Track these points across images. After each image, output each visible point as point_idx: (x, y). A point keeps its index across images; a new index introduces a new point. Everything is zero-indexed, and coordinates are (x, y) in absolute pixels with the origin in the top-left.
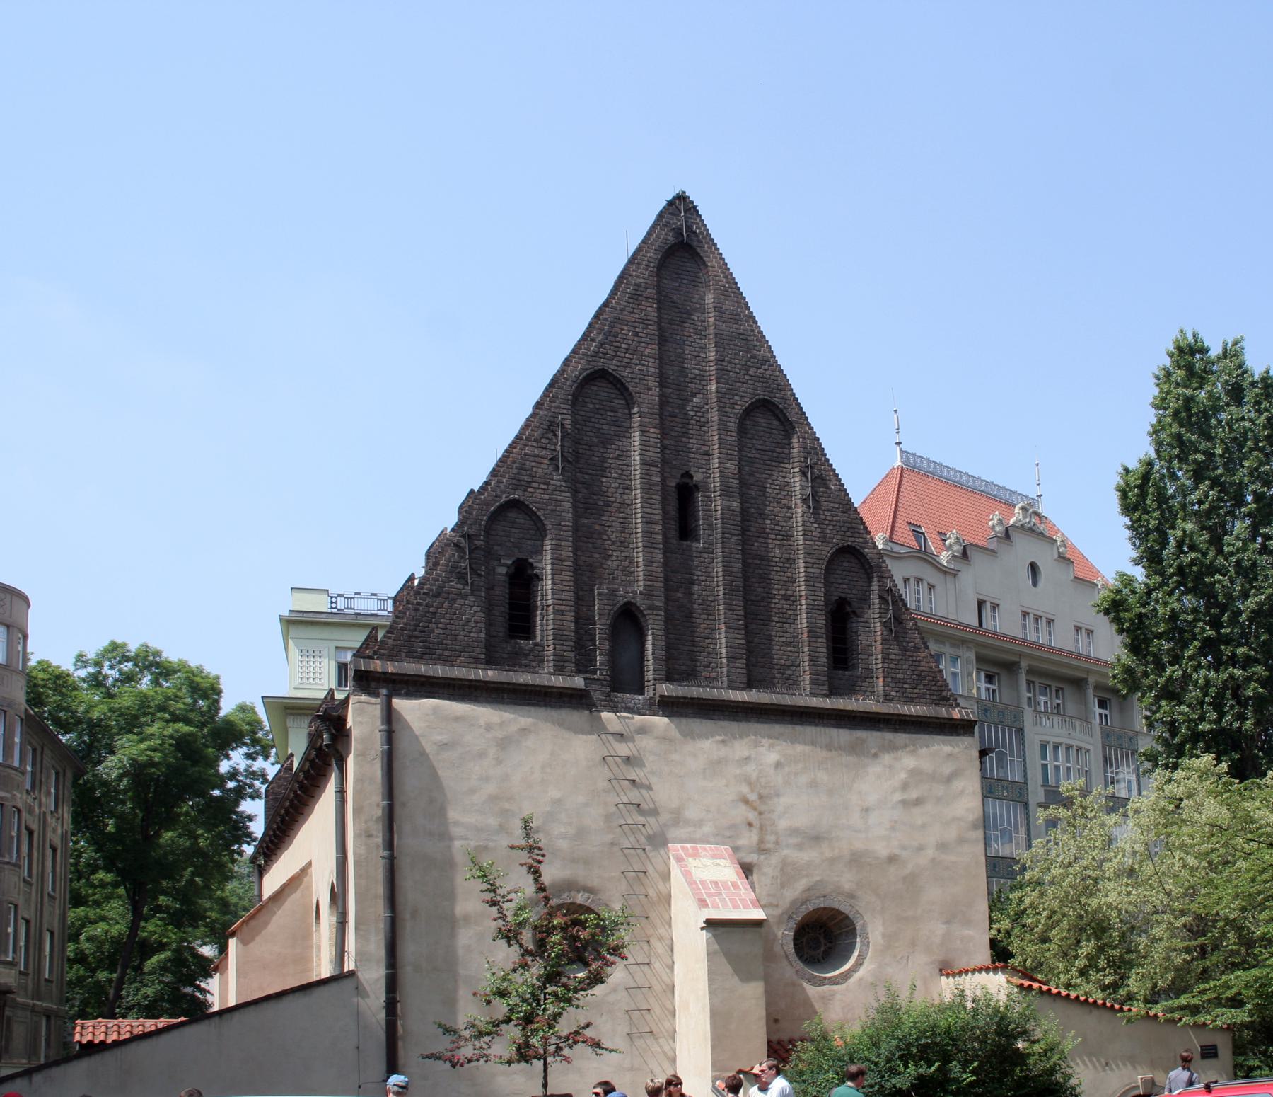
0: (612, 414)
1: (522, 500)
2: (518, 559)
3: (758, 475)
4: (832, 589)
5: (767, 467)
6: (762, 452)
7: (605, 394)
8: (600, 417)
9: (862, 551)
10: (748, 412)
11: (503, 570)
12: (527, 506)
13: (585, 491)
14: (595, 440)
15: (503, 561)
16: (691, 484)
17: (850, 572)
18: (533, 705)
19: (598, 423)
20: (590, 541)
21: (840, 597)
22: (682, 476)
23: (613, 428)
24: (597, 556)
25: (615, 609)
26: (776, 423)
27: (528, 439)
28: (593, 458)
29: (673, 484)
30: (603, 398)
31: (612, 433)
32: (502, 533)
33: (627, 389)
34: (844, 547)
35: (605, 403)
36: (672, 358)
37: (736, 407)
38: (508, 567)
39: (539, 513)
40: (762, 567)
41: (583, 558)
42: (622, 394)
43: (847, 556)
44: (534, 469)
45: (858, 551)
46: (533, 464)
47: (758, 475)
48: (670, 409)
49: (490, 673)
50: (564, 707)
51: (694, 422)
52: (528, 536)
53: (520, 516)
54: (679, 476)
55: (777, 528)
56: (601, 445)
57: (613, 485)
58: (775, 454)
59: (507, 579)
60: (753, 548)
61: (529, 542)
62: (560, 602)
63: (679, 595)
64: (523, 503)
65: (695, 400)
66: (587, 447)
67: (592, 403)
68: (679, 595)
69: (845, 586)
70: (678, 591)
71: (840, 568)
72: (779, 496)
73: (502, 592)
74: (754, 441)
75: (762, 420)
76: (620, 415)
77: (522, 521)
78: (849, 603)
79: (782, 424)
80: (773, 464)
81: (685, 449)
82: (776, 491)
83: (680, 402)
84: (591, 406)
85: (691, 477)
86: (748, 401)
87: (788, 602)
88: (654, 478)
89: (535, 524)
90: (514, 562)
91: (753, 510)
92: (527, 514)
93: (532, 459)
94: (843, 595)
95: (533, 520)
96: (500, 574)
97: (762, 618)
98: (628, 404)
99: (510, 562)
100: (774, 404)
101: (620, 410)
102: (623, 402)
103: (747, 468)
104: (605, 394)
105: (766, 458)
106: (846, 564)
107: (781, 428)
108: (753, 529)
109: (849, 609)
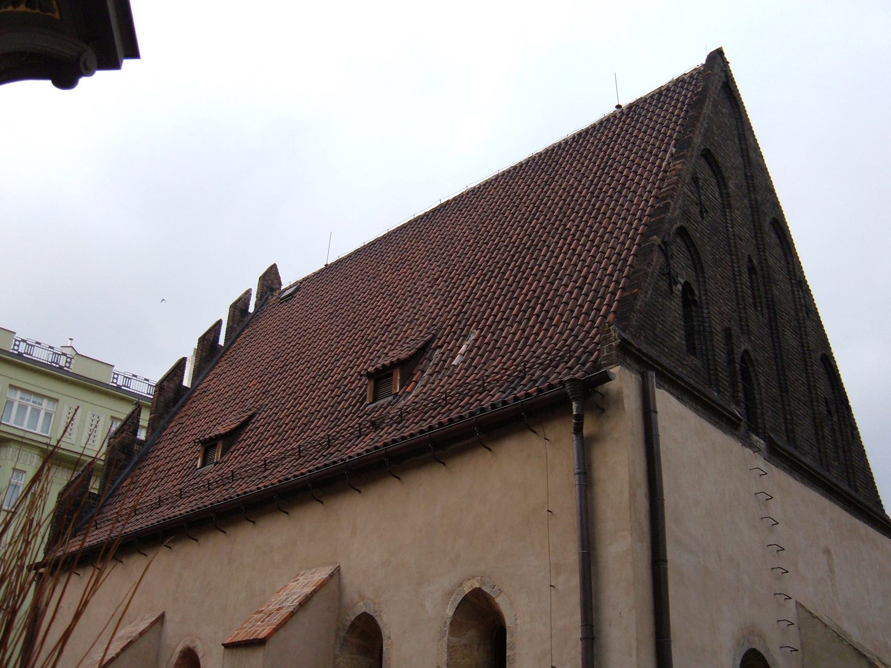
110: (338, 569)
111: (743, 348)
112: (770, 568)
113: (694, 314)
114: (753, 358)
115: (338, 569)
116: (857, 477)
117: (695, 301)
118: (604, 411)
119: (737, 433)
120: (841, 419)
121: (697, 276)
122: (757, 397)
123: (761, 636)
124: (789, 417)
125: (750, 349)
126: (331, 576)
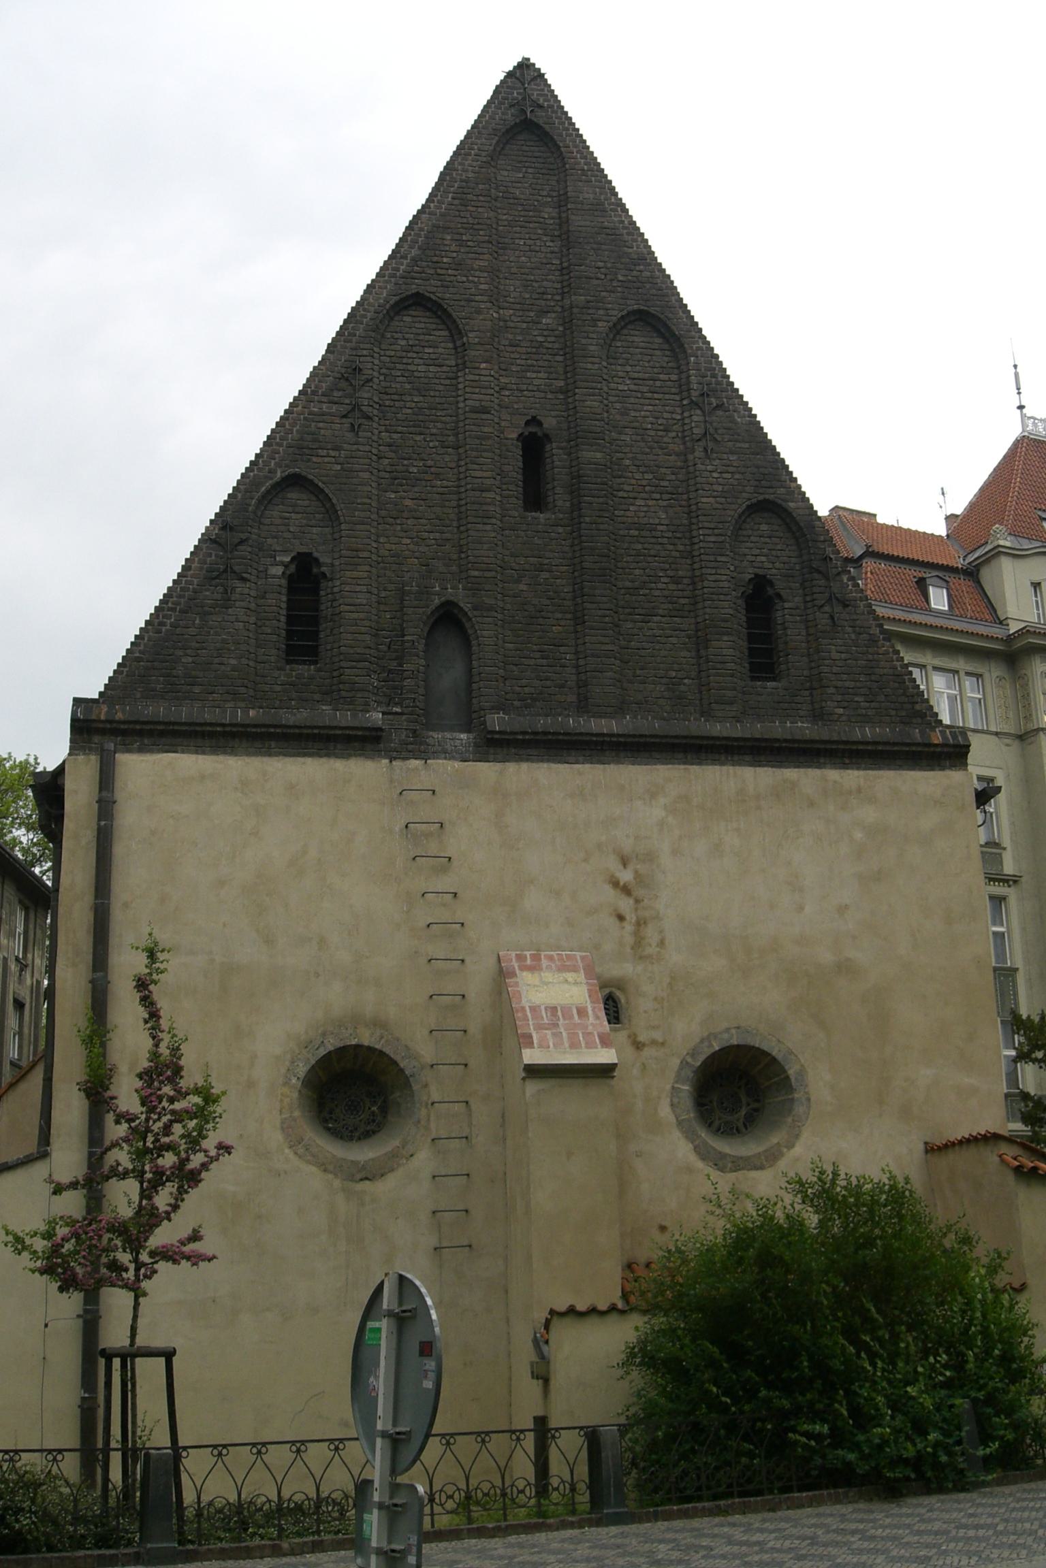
0: (431, 350)
1: (304, 474)
2: (298, 553)
3: (633, 414)
4: (745, 563)
5: (647, 401)
6: (641, 382)
7: (422, 325)
8: (415, 355)
9: (784, 504)
10: (617, 329)
11: (279, 570)
12: (311, 482)
13: (392, 455)
14: (407, 386)
15: (278, 559)
16: (540, 434)
17: (770, 537)
19: (412, 363)
20: (398, 522)
21: (756, 575)
22: (528, 423)
23: (432, 369)
24: (408, 541)
25: (429, 611)
26: (659, 340)
27: (314, 393)
28: (405, 411)
29: (515, 436)
30: (420, 331)
31: (431, 375)
32: (279, 521)
33: (450, 316)
34: (759, 502)
35: (422, 337)
36: (514, 270)
37: (600, 324)
38: (286, 566)
39: (327, 491)
40: (642, 540)
41: (388, 546)
42: (444, 323)
43: (766, 515)
44: (322, 432)
45: (780, 506)
46: (321, 425)
47: (633, 414)
48: (510, 336)
49: (252, 713)
50: (356, 756)
51: (544, 351)
52: (313, 522)
53: (304, 496)
54: (523, 423)
55: (663, 483)
56: (416, 393)
57: (431, 444)
58: (658, 383)
59: (284, 582)
60: (628, 513)
61: (315, 530)
63: (523, 587)
64: (305, 479)
65: (544, 321)
66: (396, 397)
67: (404, 339)
68: (523, 587)
69: (763, 559)
70: (518, 581)
71: (756, 533)
72: (665, 439)
73: (278, 602)
74: (629, 368)
75: (639, 338)
76: (440, 350)
77: (306, 503)
78: (771, 583)
79: (667, 341)
80: (656, 396)
81: (530, 388)
82: (660, 433)
83: (525, 325)
84: (403, 343)
85: (540, 424)
86: (616, 314)
87: (680, 586)
88: (486, 429)
89: (324, 506)
90: (293, 559)
91: (627, 462)
92: (312, 492)
93: (317, 418)
94: (760, 572)
95: (319, 500)
96: (274, 577)
97: (641, 611)
98: (452, 336)
99: (287, 559)
100: (653, 316)
101: (442, 344)
102: (446, 333)
103: (618, 406)
104: (422, 325)
105: (645, 389)
106: (764, 527)
107: (666, 346)
108: (626, 487)
109: (770, 591)
111: (437, 602)
117: (324, 574)
120: (808, 598)
123: (378, 1023)
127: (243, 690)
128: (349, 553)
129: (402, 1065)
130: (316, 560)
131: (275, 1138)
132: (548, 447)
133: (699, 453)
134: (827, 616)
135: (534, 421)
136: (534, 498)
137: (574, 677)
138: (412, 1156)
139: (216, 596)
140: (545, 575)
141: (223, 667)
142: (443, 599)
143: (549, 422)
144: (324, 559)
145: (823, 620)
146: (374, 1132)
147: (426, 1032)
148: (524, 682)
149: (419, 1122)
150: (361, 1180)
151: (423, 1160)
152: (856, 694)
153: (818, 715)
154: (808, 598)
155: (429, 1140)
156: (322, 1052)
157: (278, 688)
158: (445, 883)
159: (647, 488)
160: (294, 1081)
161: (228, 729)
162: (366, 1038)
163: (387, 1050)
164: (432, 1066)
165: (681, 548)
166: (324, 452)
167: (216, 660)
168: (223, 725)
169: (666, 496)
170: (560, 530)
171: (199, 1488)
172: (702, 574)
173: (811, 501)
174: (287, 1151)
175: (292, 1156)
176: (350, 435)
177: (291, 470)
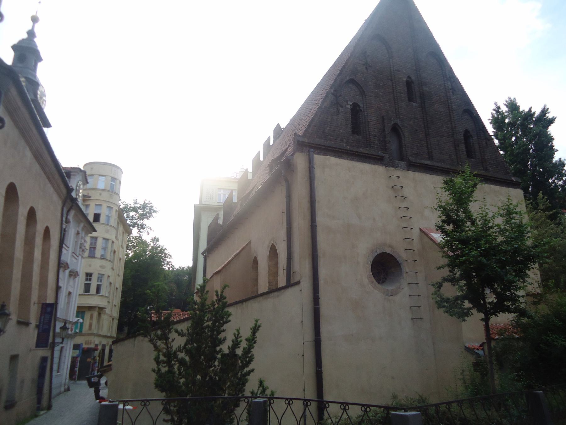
2: (354, 102)
11: (349, 107)
15: (349, 103)
18: (365, 162)
24: (382, 104)
49: (348, 147)
50: (376, 164)
61: (357, 97)
62: (371, 121)
78: (469, 132)
91: (433, 93)
96: (348, 108)
106: (466, 117)
110: (250, 242)
111: (393, 123)
112: (400, 217)
113: (360, 116)
114: (400, 126)
115: (250, 242)
116: (488, 163)
117: (361, 110)
118: (293, 171)
119: (383, 162)
121: (363, 98)
122: (403, 142)
123: (390, 246)
124: (429, 146)
125: (399, 122)
126: (247, 245)
127: (345, 140)
128: (369, 105)
129: (398, 260)
130: (359, 105)
131: (366, 281)
132: (413, 85)
133: (451, 93)
134: (485, 143)
135: (409, 77)
136: (410, 99)
137: (427, 151)
138: (403, 288)
139: (334, 110)
140: (416, 121)
141: (339, 132)
142: (394, 122)
143: (413, 78)
144: (361, 105)
145: (484, 143)
146: (385, 281)
147: (403, 250)
148: (415, 150)
149: (404, 278)
150: (390, 296)
151: (406, 290)
152: (494, 165)
153: (486, 170)
154: (479, 137)
155: (407, 284)
156: (376, 254)
157: (352, 141)
158: (405, 205)
159: (438, 101)
160: (370, 263)
161: (343, 151)
162: (388, 251)
163: (393, 255)
164: (406, 261)
165: (448, 119)
166: (359, 74)
167: (337, 130)
168: (342, 149)
169: (443, 104)
170: (419, 109)
171: (133, 421)
172: (455, 127)
173: (477, 111)
174: (370, 285)
175: (371, 287)
176: (365, 71)
177: (351, 77)
